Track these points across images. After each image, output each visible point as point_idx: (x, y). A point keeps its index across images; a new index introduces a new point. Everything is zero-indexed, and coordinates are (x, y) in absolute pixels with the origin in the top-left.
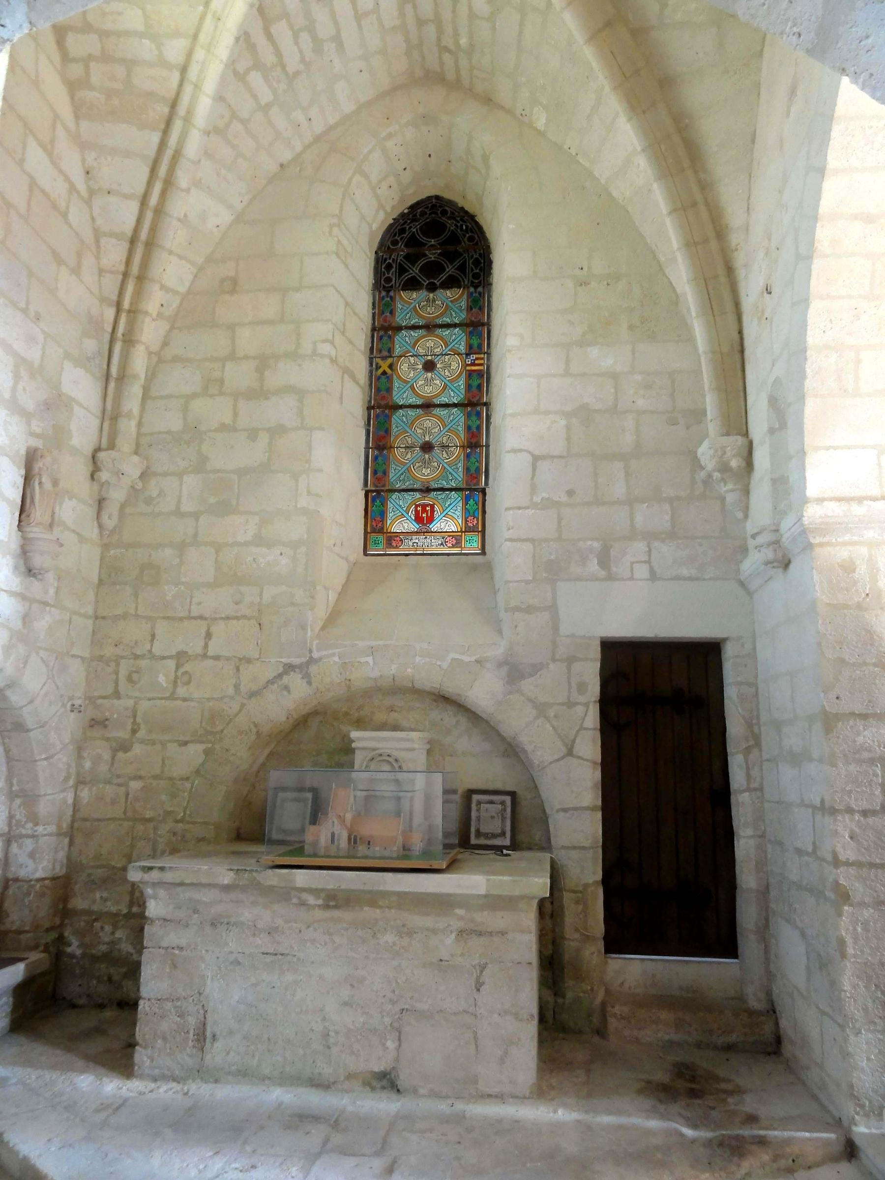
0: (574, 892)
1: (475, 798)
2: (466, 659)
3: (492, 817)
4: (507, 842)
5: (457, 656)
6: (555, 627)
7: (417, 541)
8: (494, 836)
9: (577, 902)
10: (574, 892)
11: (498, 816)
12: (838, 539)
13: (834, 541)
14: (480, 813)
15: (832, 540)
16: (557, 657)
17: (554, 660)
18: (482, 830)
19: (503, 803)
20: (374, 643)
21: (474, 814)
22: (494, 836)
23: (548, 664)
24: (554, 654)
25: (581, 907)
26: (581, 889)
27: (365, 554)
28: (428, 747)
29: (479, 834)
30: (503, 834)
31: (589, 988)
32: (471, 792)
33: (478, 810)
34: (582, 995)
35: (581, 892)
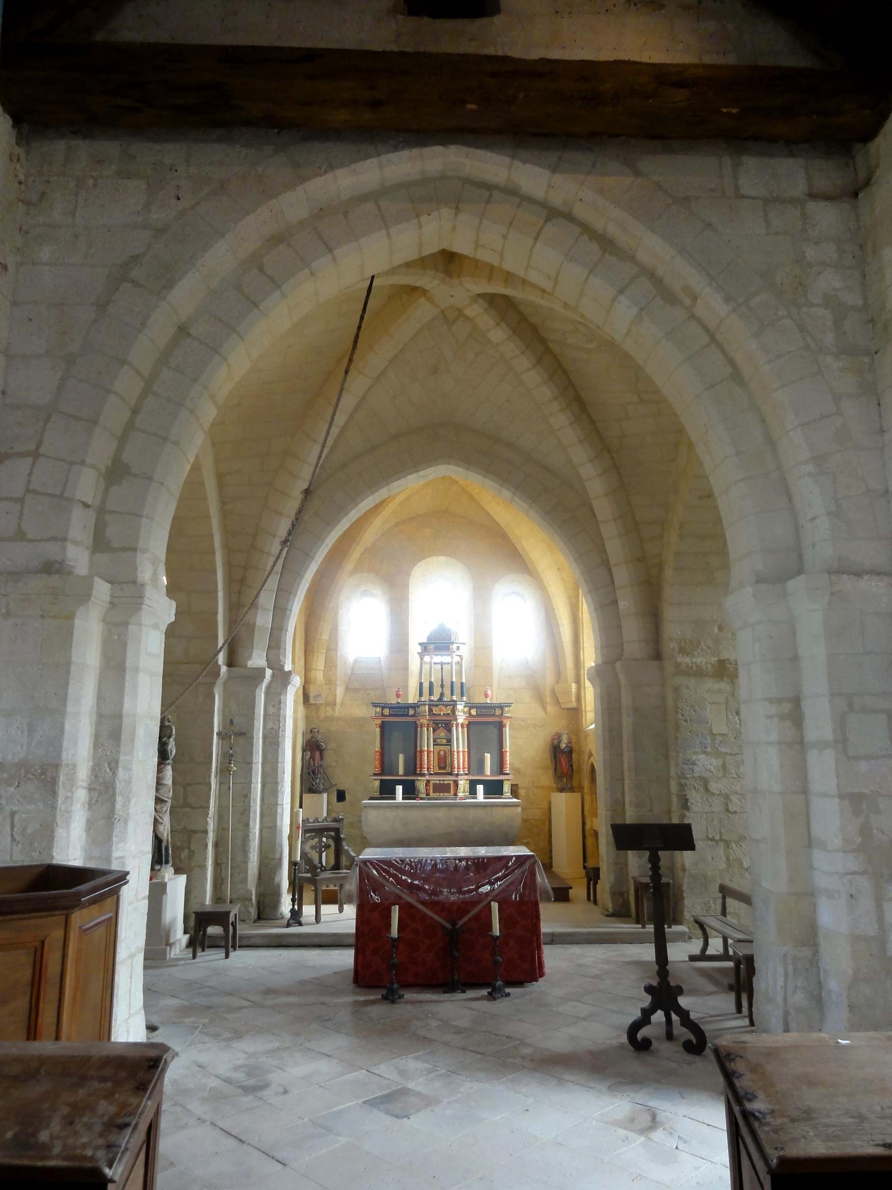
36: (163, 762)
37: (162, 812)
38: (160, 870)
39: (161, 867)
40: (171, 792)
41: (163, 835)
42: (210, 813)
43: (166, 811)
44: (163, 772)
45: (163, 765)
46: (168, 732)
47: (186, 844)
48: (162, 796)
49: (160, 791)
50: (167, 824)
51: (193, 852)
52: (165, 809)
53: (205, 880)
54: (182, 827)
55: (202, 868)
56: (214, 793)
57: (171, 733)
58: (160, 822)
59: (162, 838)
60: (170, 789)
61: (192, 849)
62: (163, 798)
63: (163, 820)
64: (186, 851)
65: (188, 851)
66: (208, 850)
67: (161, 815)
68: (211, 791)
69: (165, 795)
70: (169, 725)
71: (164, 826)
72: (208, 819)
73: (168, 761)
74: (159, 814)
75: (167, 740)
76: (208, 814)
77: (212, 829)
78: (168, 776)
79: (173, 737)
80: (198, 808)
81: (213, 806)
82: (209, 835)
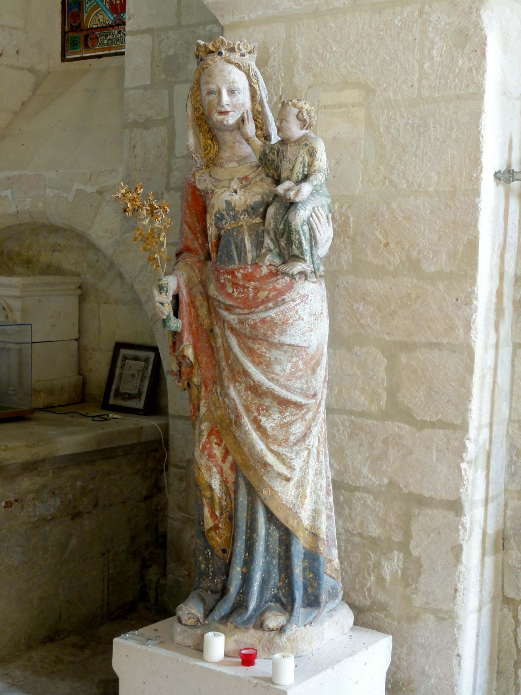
0: (180, 467)
1: (123, 352)
2: (89, 189)
3: (133, 376)
4: (140, 404)
5: (82, 187)
6: (171, 148)
7: (111, 37)
8: (131, 397)
9: (181, 479)
10: (180, 467)
11: (139, 374)
12: (251, 16)
13: (246, 18)
14: (123, 370)
15: (244, 17)
16: (172, 185)
17: (168, 188)
18: (122, 390)
19: (146, 360)
20: (11, 174)
21: (118, 370)
22: (131, 397)
23: (163, 194)
24: (168, 182)
25: (184, 485)
26: (184, 465)
27: (64, 59)
28: (79, 292)
29: (118, 394)
30: (140, 394)
31: (187, 573)
32: (119, 346)
33: (122, 367)
34: (181, 579)
35: (184, 468)
36: (284, 268)
37: (287, 440)
38: (281, 630)
39: (288, 621)
40: (322, 372)
41: (296, 516)
42: (470, 446)
43: (304, 437)
44: (284, 302)
45: (288, 279)
46: (300, 159)
47: (398, 537)
48: (288, 389)
49: (277, 368)
50: (311, 477)
51: (418, 562)
52: (298, 429)
53: (455, 661)
54: (386, 481)
55: (443, 619)
56: (489, 380)
57: (310, 165)
58: (279, 474)
59: (291, 524)
60: (318, 364)
61: (415, 553)
62: (283, 393)
63: (291, 468)
64: (397, 556)
65: (401, 556)
66: (461, 568)
67: (281, 450)
68: (470, 371)
69: (298, 384)
70: (305, 137)
71: (301, 485)
72: (463, 465)
73: (299, 267)
74: (274, 447)
75: (289, 190)
76: (463, 448)
77: (480, 495)
78: (306, 318)
79: (318, 179)
80: (433, 425)
81: (486, 420)
82: (466, 520)
